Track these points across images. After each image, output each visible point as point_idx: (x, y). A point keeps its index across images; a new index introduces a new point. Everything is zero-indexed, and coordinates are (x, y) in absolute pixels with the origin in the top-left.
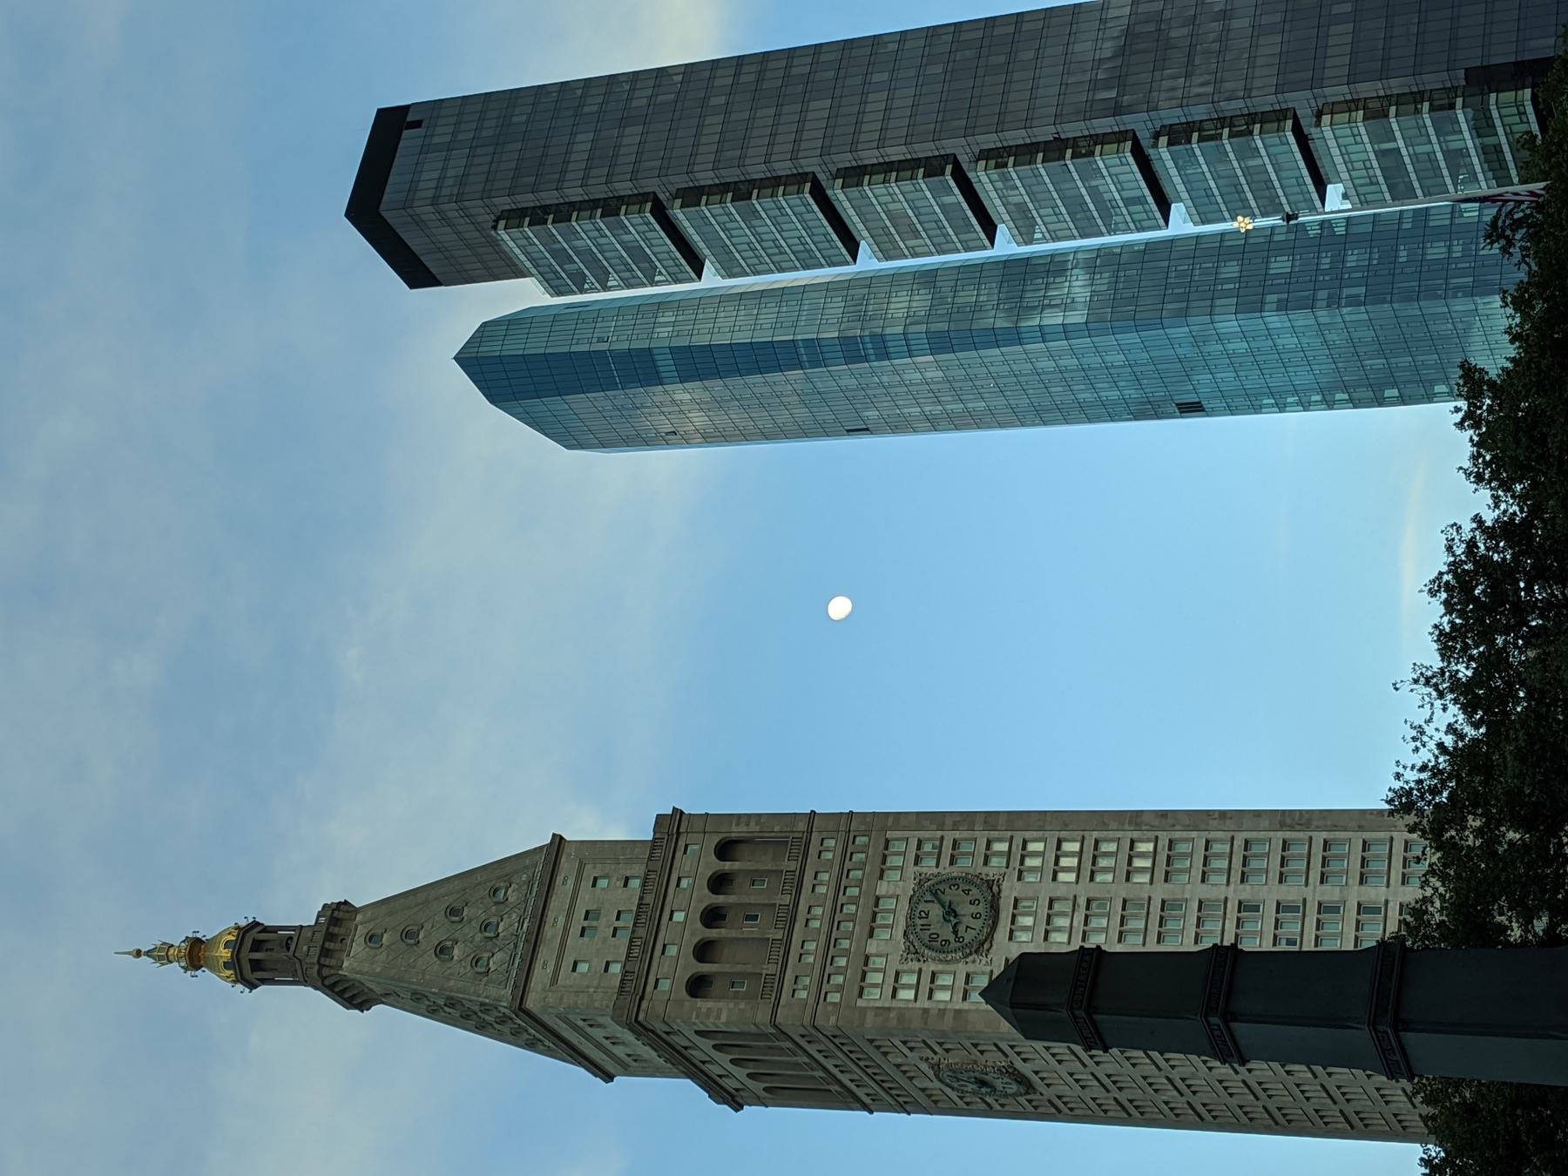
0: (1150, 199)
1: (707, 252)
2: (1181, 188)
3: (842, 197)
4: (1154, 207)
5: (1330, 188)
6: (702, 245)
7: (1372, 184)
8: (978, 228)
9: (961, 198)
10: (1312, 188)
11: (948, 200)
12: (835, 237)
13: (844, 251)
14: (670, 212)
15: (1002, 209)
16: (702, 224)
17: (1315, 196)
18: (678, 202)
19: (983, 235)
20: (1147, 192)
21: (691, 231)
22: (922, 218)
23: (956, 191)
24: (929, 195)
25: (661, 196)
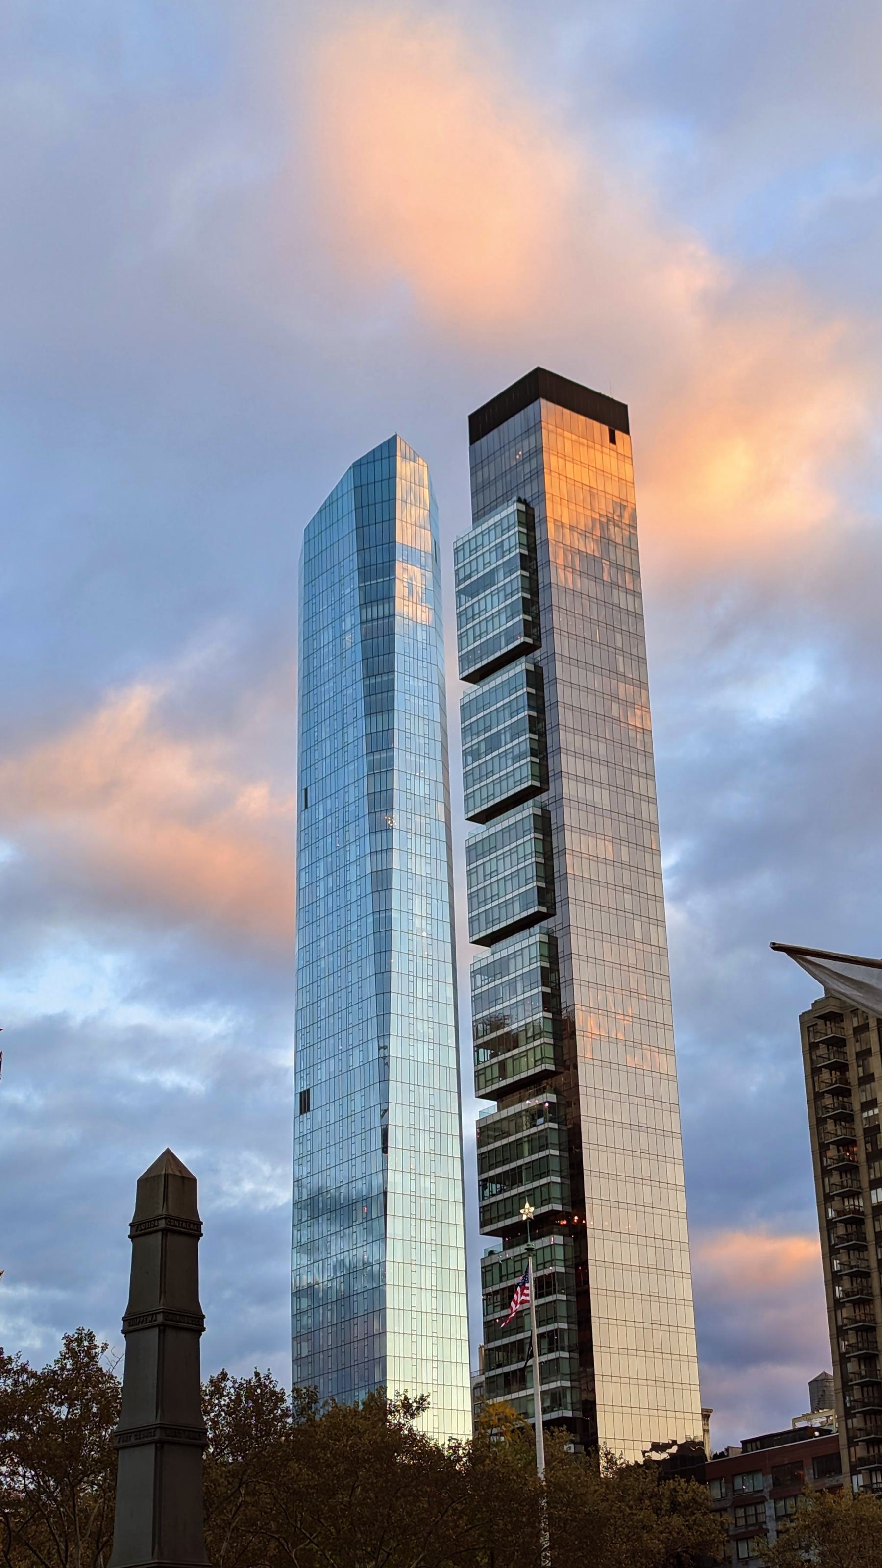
0: (503, 1083)
1: (486, 688)
2: (511, 1111)
3: (526, 813)
4: (496, 1086)
5: (500, 1240)
6: (492, 684)
7: (501, 1277)
8: (489, 931)
9: (517, 918)
10: (501, 1224)
11: (517, 905)
12: (491, 804)
13: (478, 811)
14: (523, 659)
15: (504, 953)
16: (510, 686)
17: (494, 1227)
18: (532, 668)
19: (483, 934)
20: (510, 1081)
21: (505, 677)
22: (502, 882)
23: (524, 915)
24: (522, 890)
25: (537, 653)
